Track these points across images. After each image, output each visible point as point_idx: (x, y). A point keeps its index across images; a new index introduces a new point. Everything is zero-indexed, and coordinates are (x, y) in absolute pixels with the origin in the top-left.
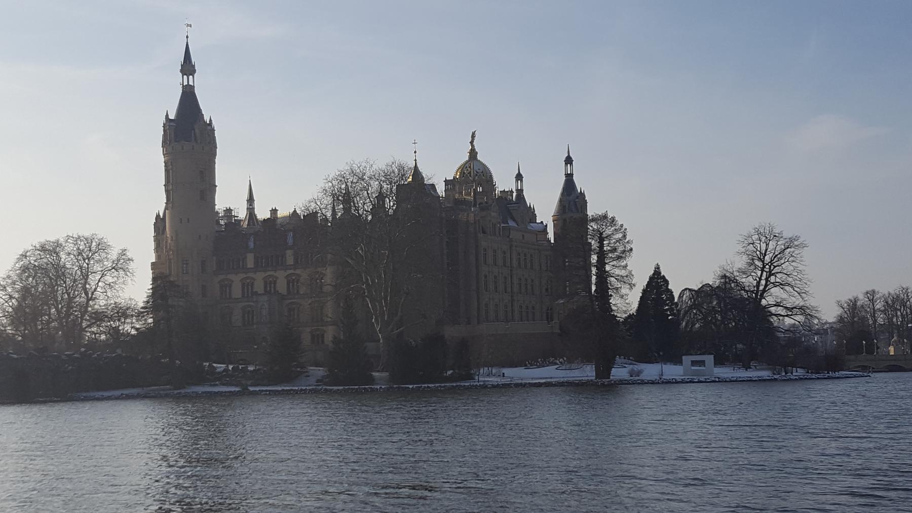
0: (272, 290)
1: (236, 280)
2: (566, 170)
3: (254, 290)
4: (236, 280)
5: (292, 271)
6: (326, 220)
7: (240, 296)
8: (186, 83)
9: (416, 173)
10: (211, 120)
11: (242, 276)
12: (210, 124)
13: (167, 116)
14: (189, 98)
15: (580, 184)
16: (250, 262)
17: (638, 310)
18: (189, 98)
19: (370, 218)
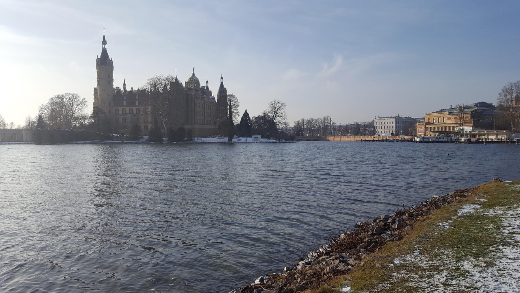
0: (132, 112)
1: (120, 109)
2: (221, 81)
3: (126, 112)
4: (120, 109)
5: (138, 107)
6: (148, 92)
7: (121, 114)
8: (103, 47)
9: (176, 79)
10: (112, 59)
11: (123, 108)
12: (111, 60)
13: (98, 57)
14: (104, 52)
15: (225, 85)
16: (125, 103)
17: (240, 122)
18: (104, 52)
19: (162, 92)
